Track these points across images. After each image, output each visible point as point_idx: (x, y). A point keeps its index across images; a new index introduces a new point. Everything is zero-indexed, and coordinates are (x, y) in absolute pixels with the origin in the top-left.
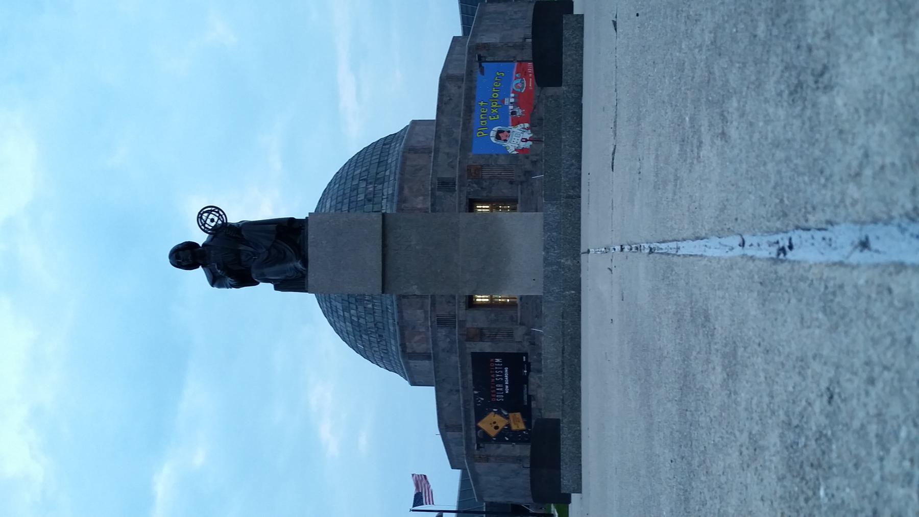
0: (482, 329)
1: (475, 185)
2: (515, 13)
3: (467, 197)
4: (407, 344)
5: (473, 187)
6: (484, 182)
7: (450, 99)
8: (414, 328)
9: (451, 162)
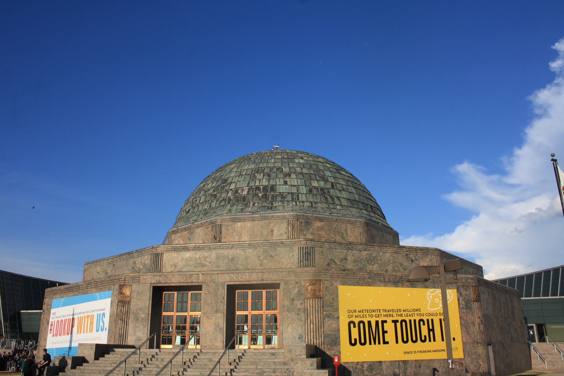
0: (129, 303)
1: (297, 290)
2: (516, 330)
4: (178, 235)
5: (294, 288)
6: (301, 301)
7: (413, 261)
9: (336, 263)
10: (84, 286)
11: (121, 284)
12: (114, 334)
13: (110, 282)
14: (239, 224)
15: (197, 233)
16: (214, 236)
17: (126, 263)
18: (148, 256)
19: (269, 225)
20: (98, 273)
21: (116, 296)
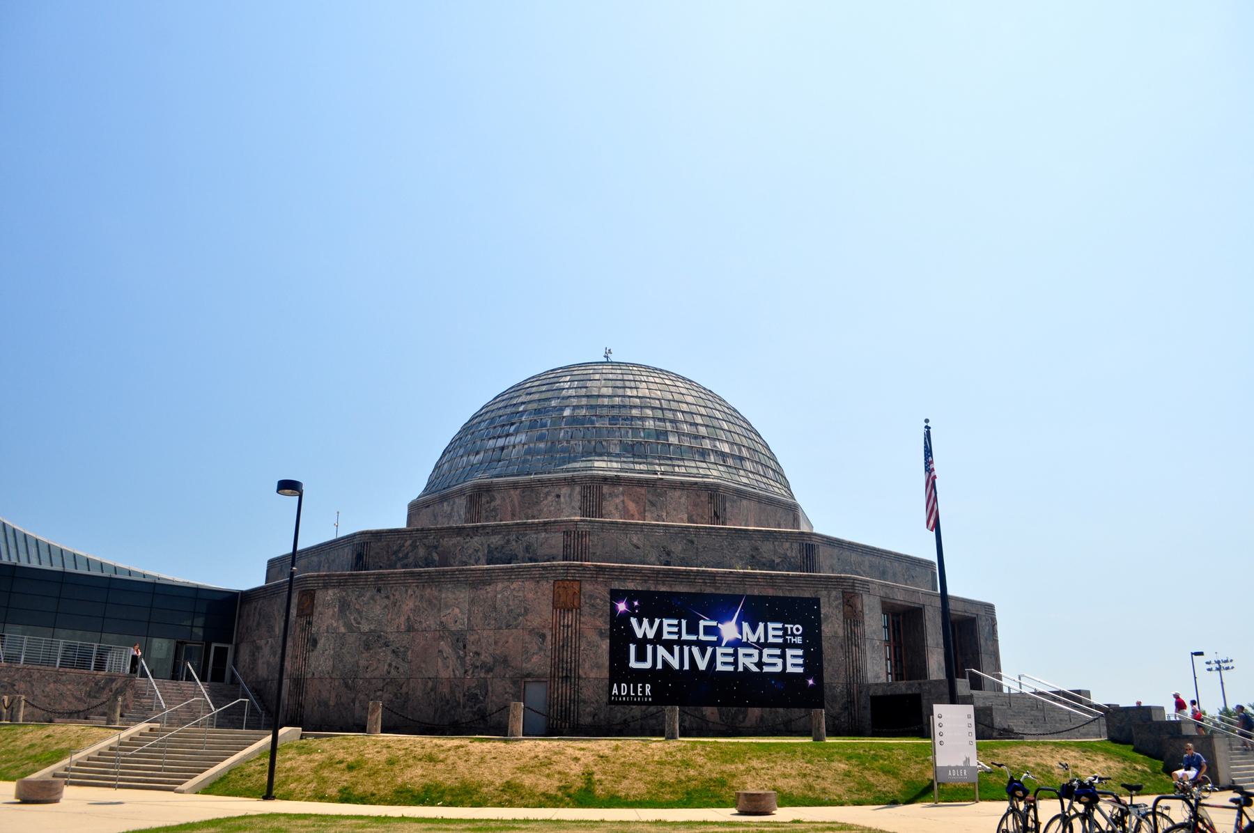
3: (977, 615)
4: (621, 489)
8: (653, 504)
10: (731, 579)
11: (846, 590)
12: (844, 667)
13: (814, 582)
14: (745, 502)
15: (672, 498)
16: (715, 513)
17: (730, 544)
18: (792, 545)
19: (776, 515)
20: (638, 548)
21: (837, 607)
